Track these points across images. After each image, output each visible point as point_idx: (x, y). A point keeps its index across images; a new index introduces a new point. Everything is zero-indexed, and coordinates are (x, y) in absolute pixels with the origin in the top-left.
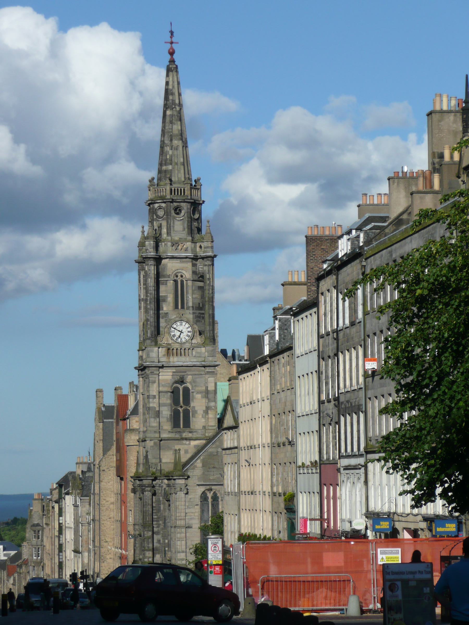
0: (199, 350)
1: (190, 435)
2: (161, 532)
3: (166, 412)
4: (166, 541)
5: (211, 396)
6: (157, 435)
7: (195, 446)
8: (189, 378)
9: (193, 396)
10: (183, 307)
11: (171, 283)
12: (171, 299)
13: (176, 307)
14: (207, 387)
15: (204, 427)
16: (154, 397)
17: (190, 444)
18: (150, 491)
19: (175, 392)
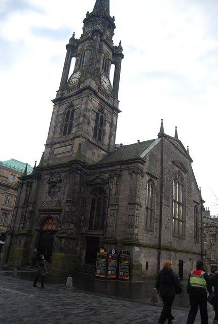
0: (111, 98)
1: (102, 146)
2: (79, 210)
3: (93, 124)
4: (83, 218)
5: (114, 127)
6: (87, 136)
7: (103, 154)
8: (106, 111)
9: (105, 123)
10: (105, 71)
11: (103, 55)
12: (102, 62)
13: (103, 69)
14: (112, 122)
15: (109, 145)
16: (90, 110)
17: (101, 152)
18: (80, 174)
19: (97, 115)
